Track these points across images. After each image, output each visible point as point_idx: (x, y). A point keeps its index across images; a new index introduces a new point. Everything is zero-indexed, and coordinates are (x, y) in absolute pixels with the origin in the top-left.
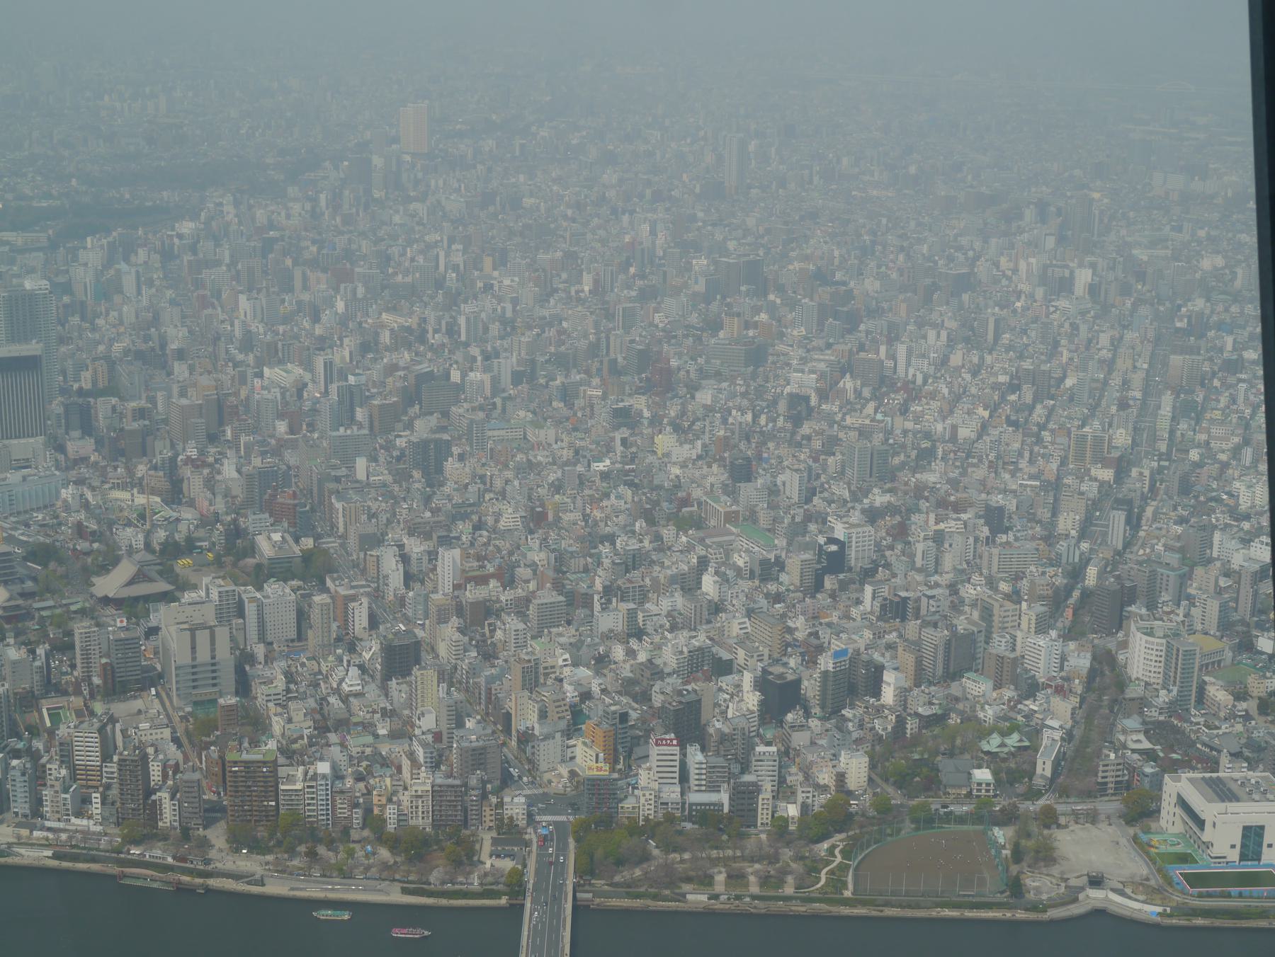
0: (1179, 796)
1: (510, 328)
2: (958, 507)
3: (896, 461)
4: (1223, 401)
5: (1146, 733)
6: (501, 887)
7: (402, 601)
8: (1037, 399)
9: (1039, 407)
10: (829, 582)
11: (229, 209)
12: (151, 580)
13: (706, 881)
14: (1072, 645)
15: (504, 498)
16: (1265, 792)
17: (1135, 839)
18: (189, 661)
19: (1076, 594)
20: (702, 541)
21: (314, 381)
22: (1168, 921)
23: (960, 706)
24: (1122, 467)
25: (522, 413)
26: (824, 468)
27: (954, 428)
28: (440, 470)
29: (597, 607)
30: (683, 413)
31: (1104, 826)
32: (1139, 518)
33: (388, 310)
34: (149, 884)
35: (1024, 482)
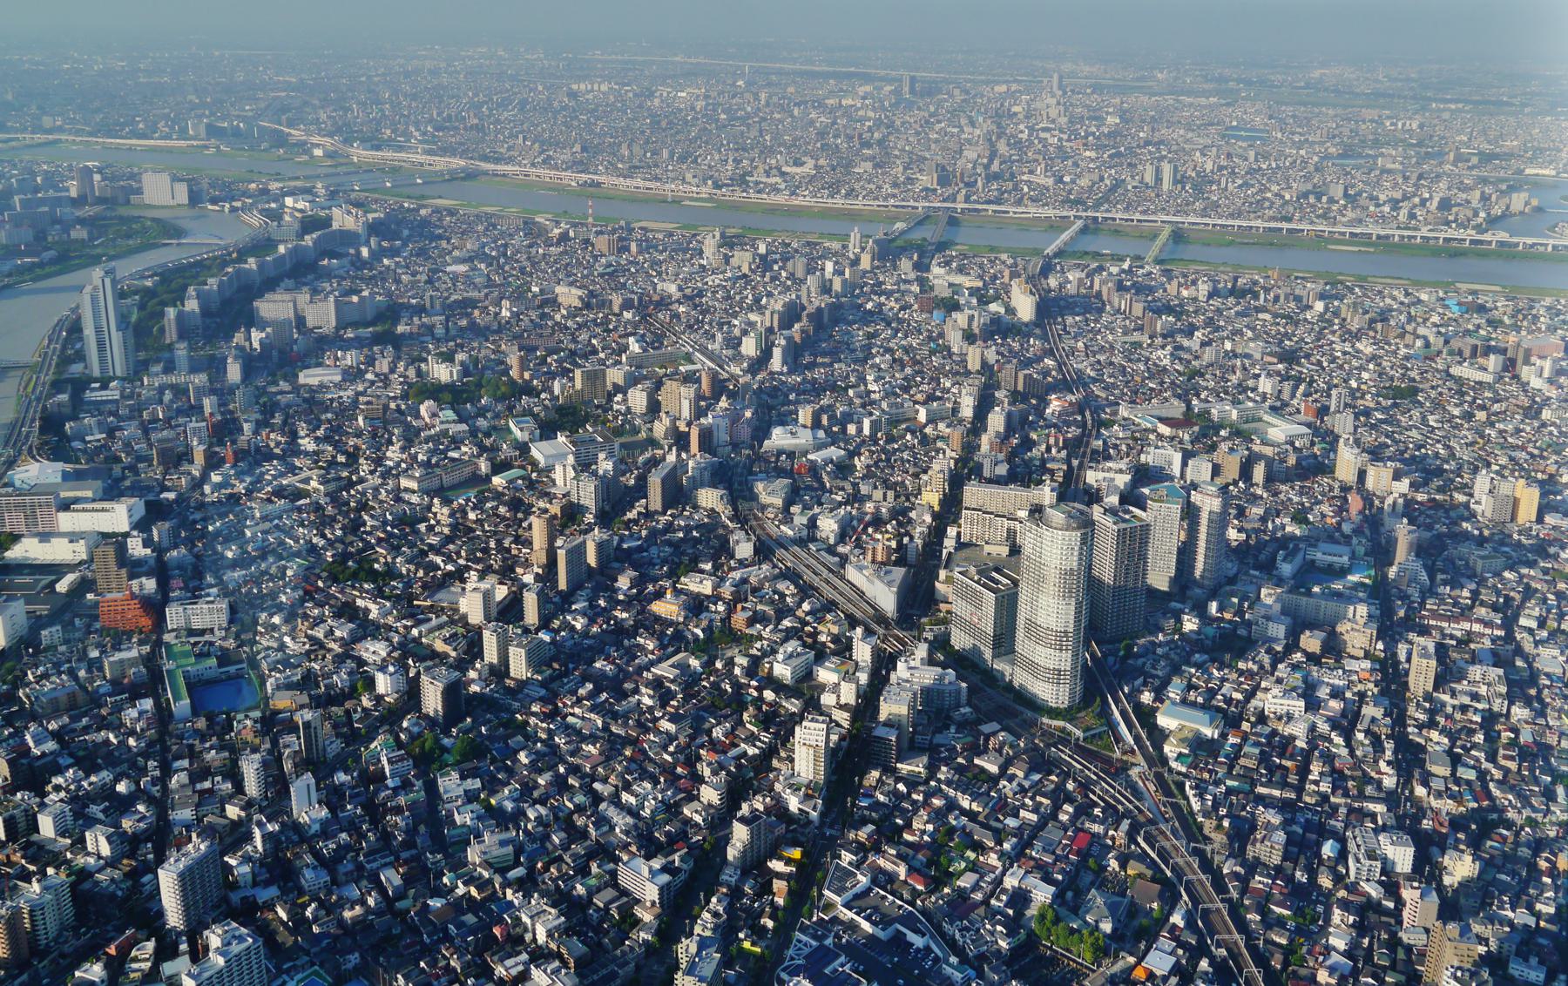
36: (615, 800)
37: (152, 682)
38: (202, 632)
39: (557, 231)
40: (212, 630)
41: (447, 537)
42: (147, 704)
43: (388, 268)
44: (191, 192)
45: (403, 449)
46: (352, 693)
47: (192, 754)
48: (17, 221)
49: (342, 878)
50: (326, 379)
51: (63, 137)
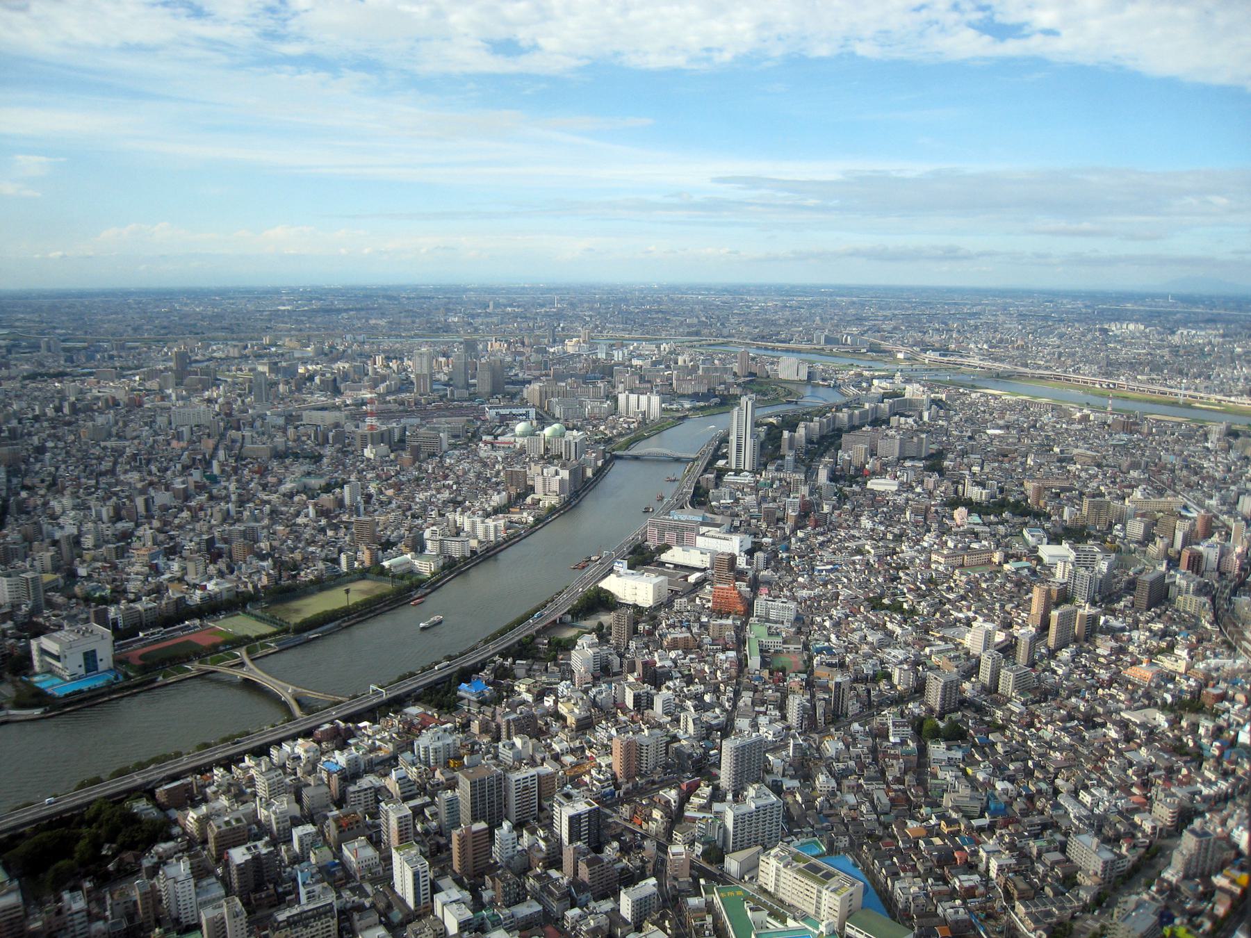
36: (1075, 794)
37: (740, 643)
38: (776, 622)
39: (1078, 415)
40: (783, 623)
41: (962, 596)
42: (732, 654)
43: (942, 426)
44: (809, 373)
45: (938, 537)
46: (875, 679)
47: (755, 690)
48: (699, 380)
49: (845, 789)
50: (888, 488)
51: (734, 340)
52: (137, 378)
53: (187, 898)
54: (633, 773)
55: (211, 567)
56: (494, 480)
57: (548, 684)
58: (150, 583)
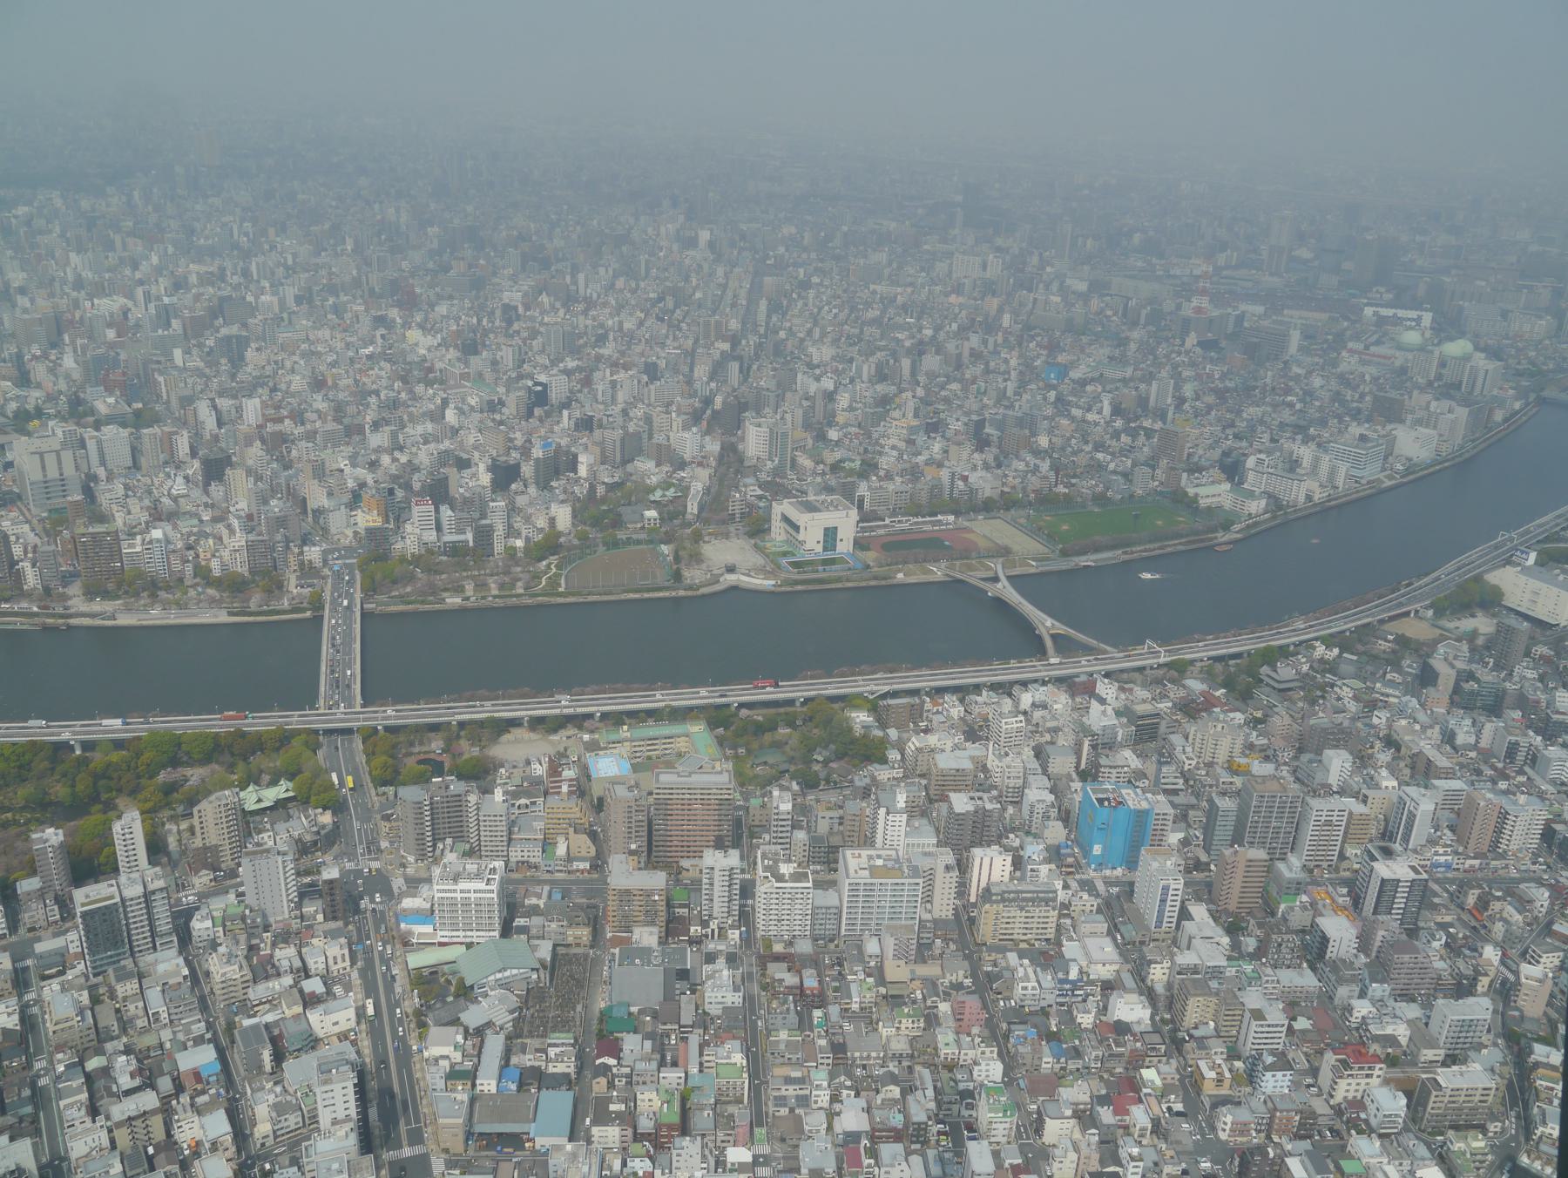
0: (783, 514)
1: (290, 271)
2: (626, 367)
3: (581, 341)
4: (800, 304)
5: (760, 487)
6: (305, 605)
7: (216, 438)
8: (676, 307)
9: (678, 311)
10: (537, 411)
11: (58, 202)
12: (6, 433)
13: (459, 590)
14: (707, 438)
15: (293, 372)
16: (836, 507)
17: (755, 545)
18: (38, 476)
19: (709, 412)
20: (445, 391)
21: (136, 306)
22: (779, 589)
23: (634, 478)
24: (735, 341)
25: (304, 322)
26: (531, 348)
27: (621, 323)
28: (242, 358)
29: (368, 431)
30: (426, 319)
31: (735, 540)
32: (749, 368)
33: (193, 262)
34: (18, 627)
35: (672, 350)
52: (920, 211)
53: (896, 834)
54: (1485, 849)
55: (976, 455)
56: (1355, 405)
57: (1382, 694)
58: (905, 461)
